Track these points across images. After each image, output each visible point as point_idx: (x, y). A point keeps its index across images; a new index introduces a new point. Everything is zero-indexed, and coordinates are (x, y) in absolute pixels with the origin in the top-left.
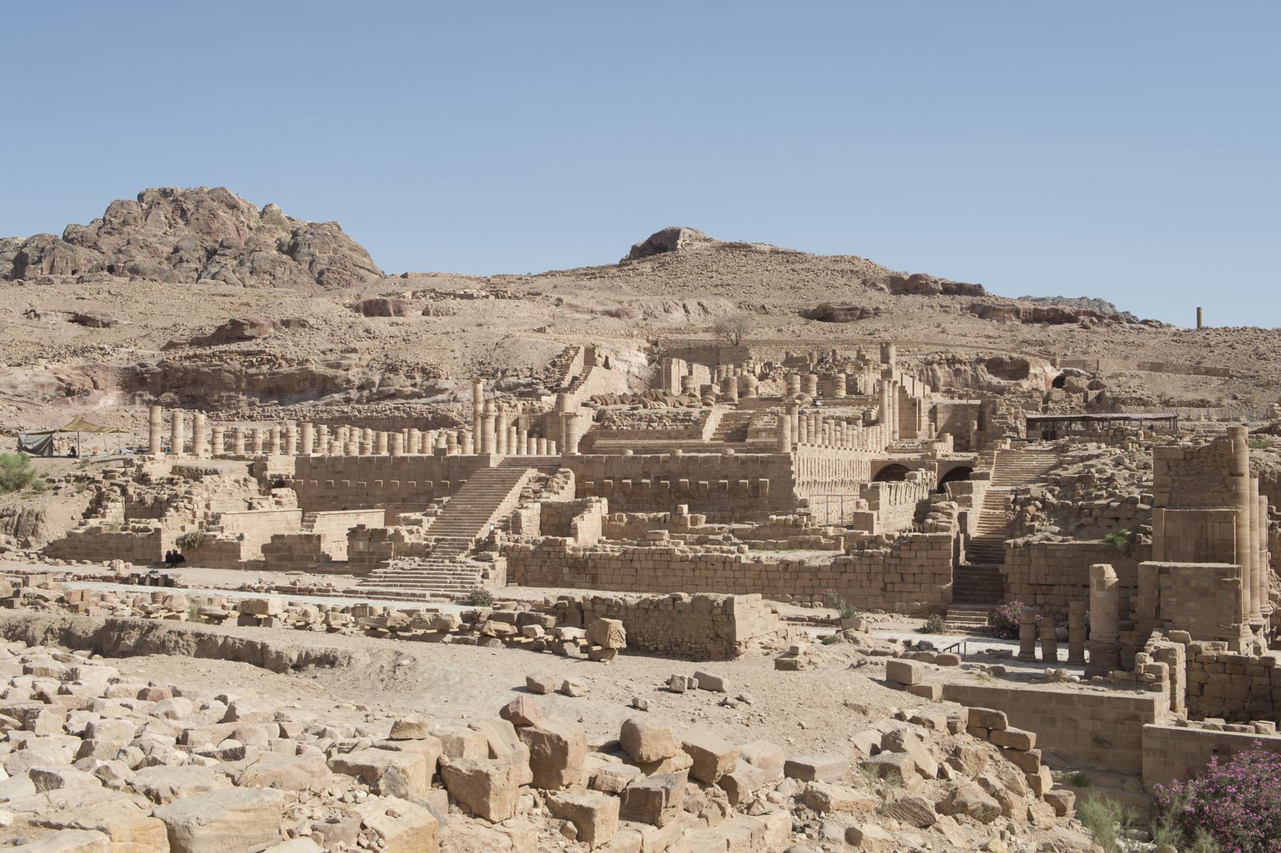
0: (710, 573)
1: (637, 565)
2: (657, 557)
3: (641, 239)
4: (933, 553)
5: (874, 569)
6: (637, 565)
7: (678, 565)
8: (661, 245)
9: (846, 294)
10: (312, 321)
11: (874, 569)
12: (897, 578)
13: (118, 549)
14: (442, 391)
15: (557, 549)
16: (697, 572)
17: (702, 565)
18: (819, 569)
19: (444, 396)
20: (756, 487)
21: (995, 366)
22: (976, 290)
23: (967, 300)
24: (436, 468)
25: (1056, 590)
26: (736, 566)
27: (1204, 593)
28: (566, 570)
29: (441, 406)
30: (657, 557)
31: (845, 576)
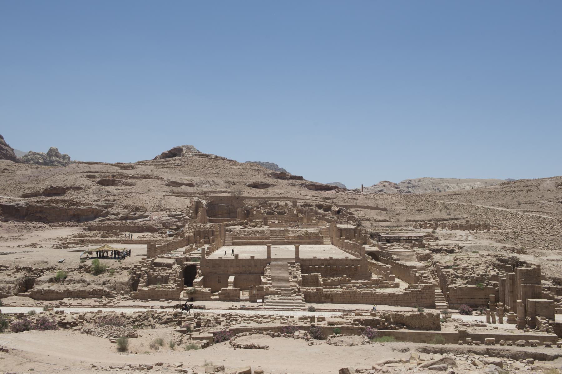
0: (367, 297)
1: (345, 296)
3: (166, 150)
4: (430, 290)
5: (414, 295)
6: (345, 296)
7: (358, 295)
8: (175, 152)
9: (259, 178)
10: (83, 187)
11: (414, 295)
12: (420, 297)
13: (162, 295)
14: (147, 217)
18: (398, 295)
19: (148, 218)
20: (356, 268)
21: (320, 207)
22: (301, 178)
23: (300, 182)
24: (252, 262)
25: (463, 300)
26: (375, 295)
27: (547, 307)
28: (323, 298)
29: (148, 222)
31: (406, 297)
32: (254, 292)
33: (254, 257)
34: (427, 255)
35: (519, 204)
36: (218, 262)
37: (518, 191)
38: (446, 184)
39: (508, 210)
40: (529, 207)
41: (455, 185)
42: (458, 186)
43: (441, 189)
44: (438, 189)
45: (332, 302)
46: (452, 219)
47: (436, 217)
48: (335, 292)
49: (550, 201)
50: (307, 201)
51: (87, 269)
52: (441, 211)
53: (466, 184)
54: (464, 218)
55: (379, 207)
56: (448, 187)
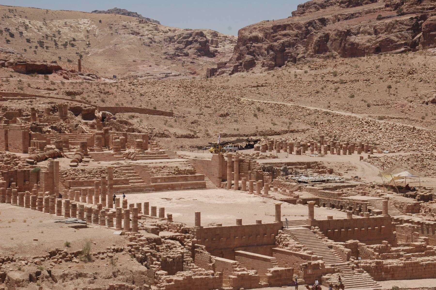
1: (407, 269)
2: (413, 265)
7: (420, 268)
15: (380, 265)
16: (426, 270)
17: (427, 267)
28: (383, 273)
30: (413, 265)
32: (310, 271)
33: (260, 222)
34: (415, 205)
35: (369, 106)
36: (218, 232)
37: (352, 81)
38: (21, 20)
39: (353, 115)
40: (383, 111)
41: (40, 23)
42: (45, 24)
43: (13, 31)
44: (7, 30)
45: (393, 278)
46: (286, 132)
47: (260, 129)
48: (395, 265)
49: (411, 102)
50: (54, 100)
51: (64, 257)
52: (255, 115)
53: (62, 22)
54: (304, 131)
55: (158, 109)
56: (26, 27)
